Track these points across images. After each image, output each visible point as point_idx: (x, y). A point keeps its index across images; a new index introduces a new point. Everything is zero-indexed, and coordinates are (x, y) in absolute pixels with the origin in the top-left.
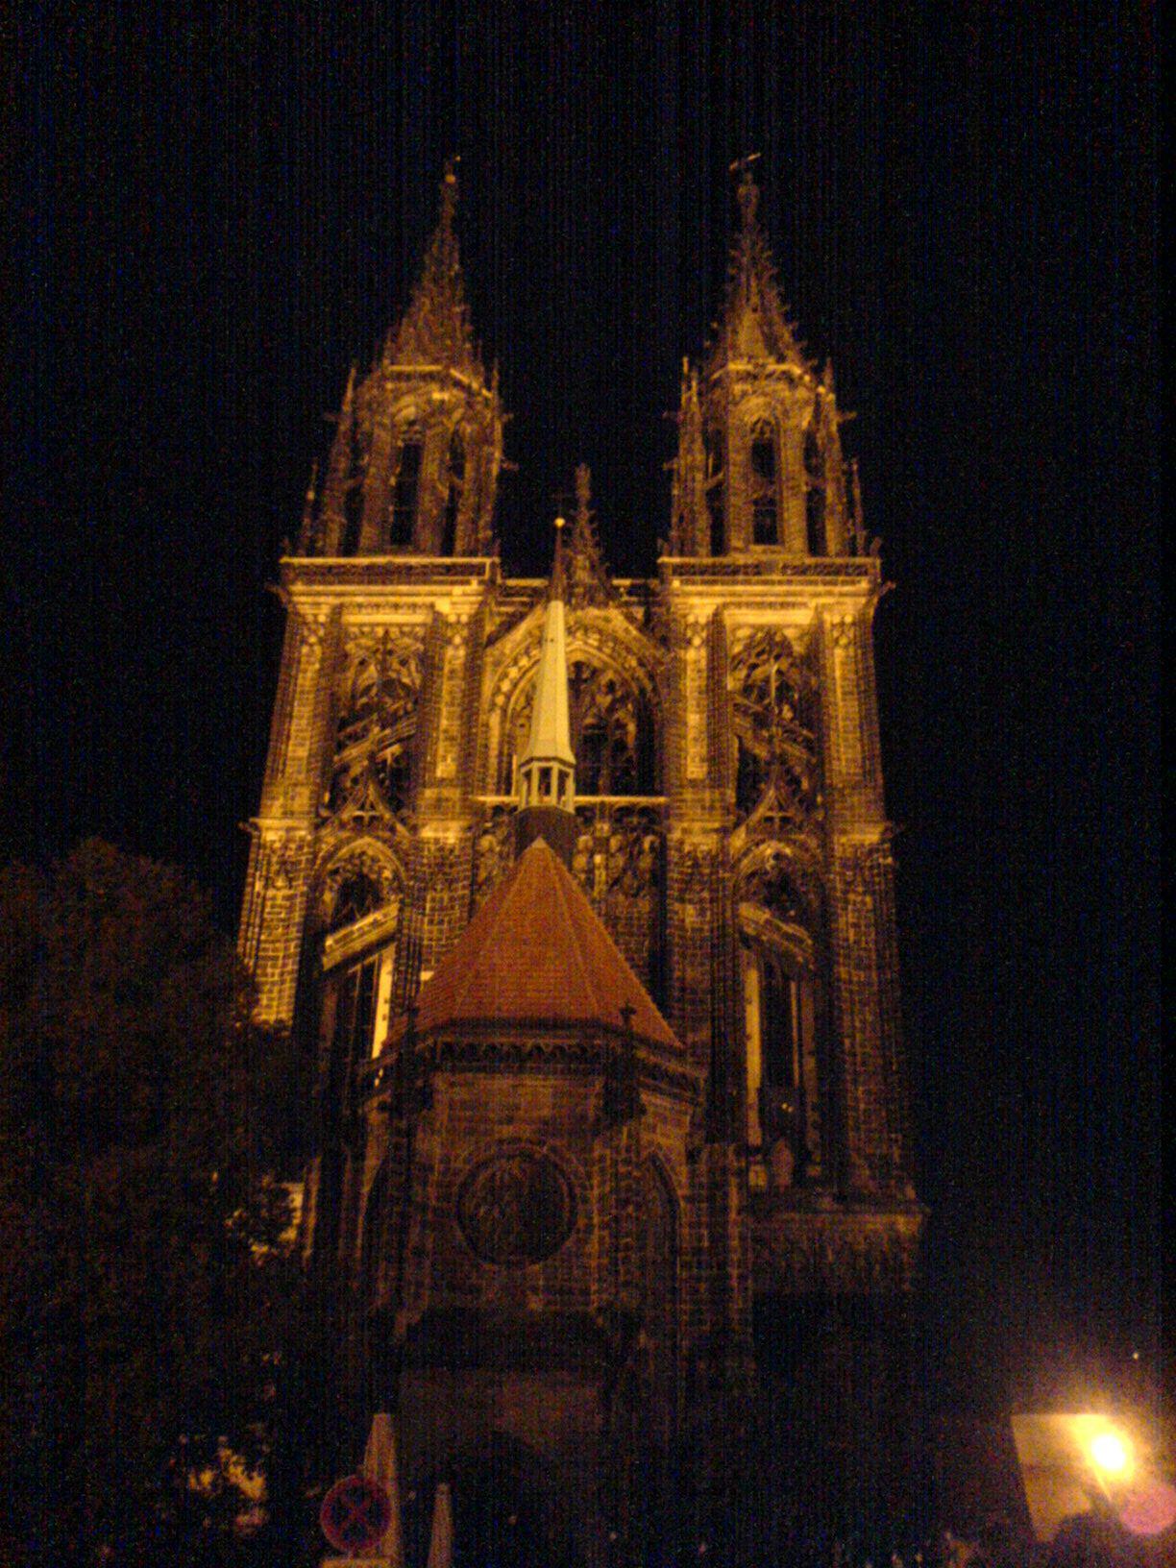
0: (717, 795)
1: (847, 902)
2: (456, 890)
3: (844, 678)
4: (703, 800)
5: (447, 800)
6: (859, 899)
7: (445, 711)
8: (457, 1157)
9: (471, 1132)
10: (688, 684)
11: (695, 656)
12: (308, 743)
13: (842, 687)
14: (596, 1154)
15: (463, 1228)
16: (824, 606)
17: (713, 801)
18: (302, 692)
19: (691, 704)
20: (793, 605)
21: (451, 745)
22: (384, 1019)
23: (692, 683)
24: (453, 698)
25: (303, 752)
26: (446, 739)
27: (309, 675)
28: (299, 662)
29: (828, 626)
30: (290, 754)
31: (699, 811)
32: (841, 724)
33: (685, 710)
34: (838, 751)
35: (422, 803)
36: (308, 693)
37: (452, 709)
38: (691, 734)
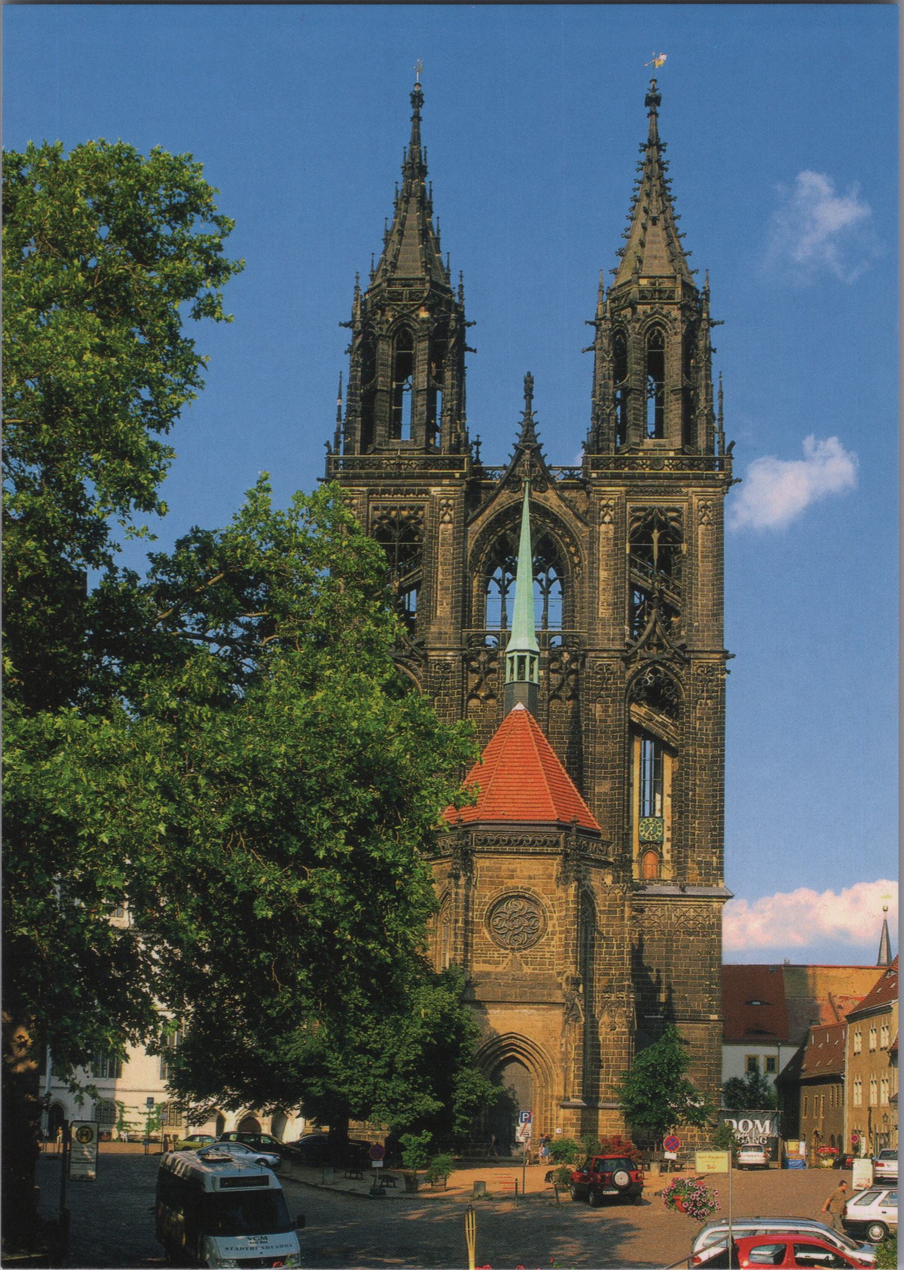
0: (617, 631)
1: (696, 703)
2: (453, 694)
4: (609, 634)
5: (446, 633)
7: (440, 568)
9: (492, 883)
10: (601, 549)
11: (606, 530)
15: (490, 932)
19: (602, 563)
23: (603, 548)
26: (441, 590)
29: (695, 507)
31: (606, 642)
34: (697, 599)
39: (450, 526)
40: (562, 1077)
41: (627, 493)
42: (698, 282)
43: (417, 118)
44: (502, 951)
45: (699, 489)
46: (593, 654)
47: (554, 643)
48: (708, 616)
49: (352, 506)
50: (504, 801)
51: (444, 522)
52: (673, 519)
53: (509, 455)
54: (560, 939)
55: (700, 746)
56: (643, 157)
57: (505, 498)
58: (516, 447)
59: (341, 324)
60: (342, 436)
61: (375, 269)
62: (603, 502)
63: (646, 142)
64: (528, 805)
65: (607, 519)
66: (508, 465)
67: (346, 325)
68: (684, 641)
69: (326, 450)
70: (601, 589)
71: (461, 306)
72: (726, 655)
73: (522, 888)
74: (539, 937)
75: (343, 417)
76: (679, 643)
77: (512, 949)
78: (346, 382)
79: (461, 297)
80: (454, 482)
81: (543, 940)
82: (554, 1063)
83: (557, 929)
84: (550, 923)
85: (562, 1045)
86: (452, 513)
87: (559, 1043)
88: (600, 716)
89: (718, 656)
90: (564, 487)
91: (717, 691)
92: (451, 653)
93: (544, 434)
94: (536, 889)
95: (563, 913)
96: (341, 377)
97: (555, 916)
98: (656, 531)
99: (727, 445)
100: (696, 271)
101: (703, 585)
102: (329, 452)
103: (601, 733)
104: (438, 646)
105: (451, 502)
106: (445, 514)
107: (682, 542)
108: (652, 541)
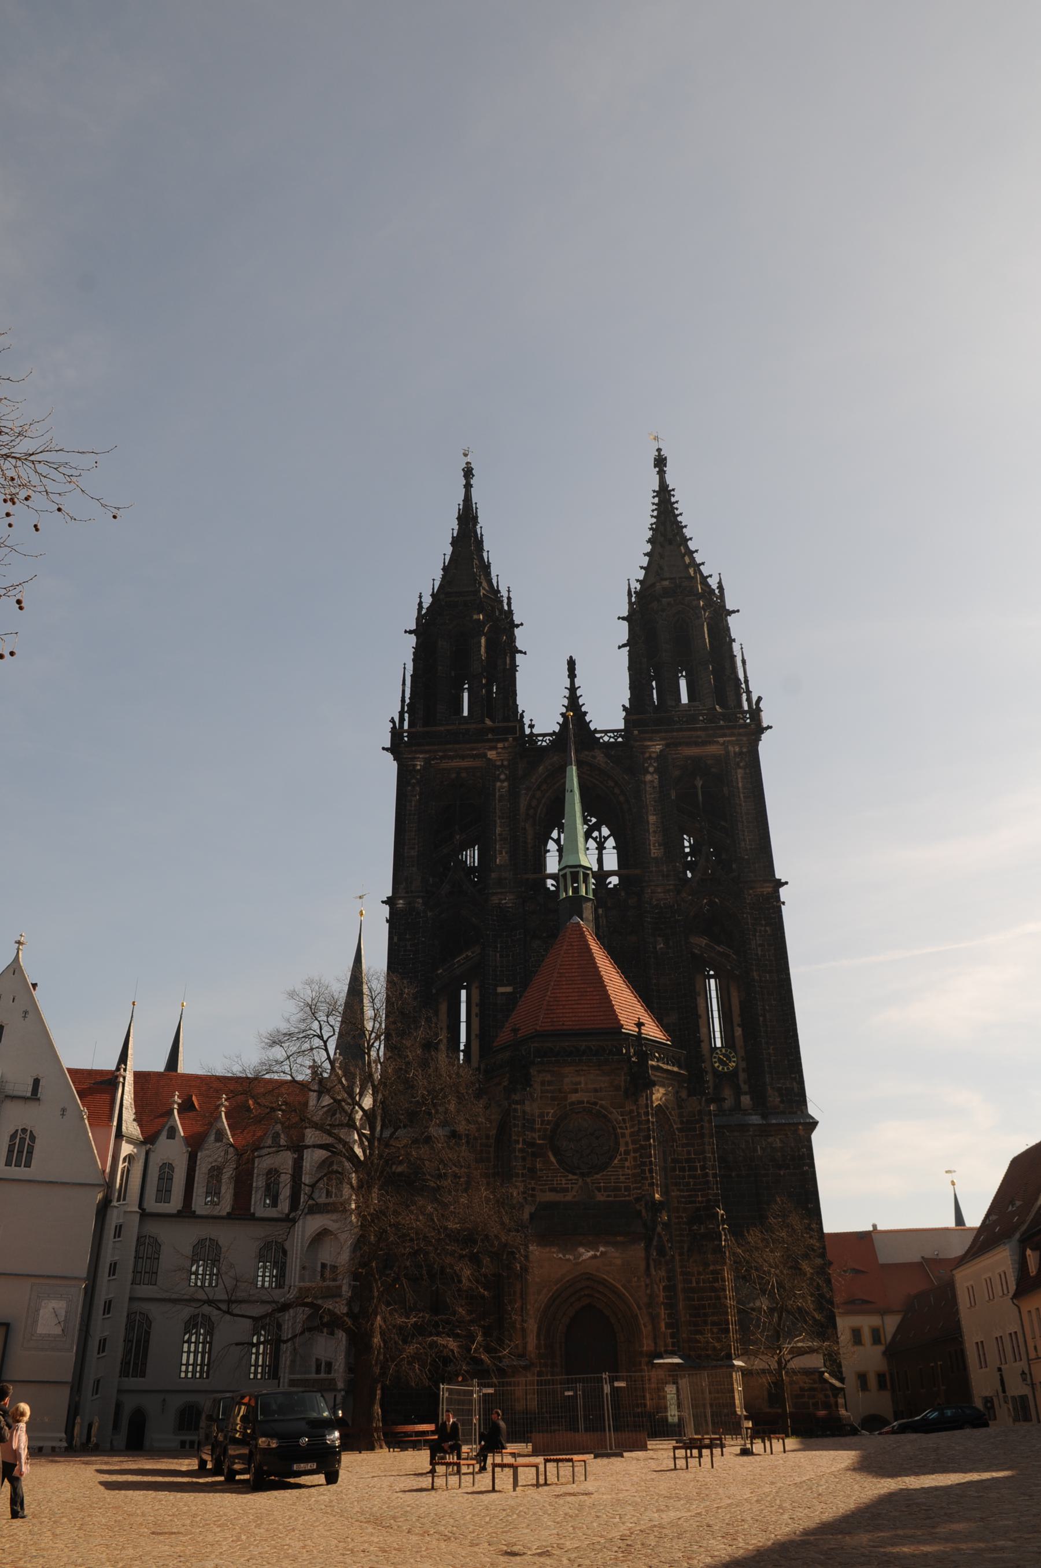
6: (763, 929)
7: (498, 821)
8: (548, 1113)
12: (417, 846)
13: (744, 793)
14: (627, 1109)
15: (555, 1156)
16: (729, 741)
19: (651, 808)
20: (710, 743)
22: (477, 1016)
23: (650, 797)
25: (414, 853)
27: (413, 803)
34: (744, 835)
37: (503, 821)
39: (505, 784)
40: (650, 1327)
41: (667, 745)
42: (713, 583)
43: (468, 486)
44: (571, 1177)
45: (734, 739)
47: (610, 883)
50: (564, 1011)
53: (558, 723)
54: (635, 1159)
56: (656, 500)
58: (563, 715)
59: (406, 632)
60: (406, 715)
61: (435, 591)
62: (647, 755)
63: (657, 489)
64: (589, 1014)
65: (651, 769)
66: (557, 731)
67: (410, 632)
69: (391, 725)
71: (510, 612)
72: (780, 884)
73: (588, 1102)
74: (612, 1158)
75: (407, 701)
77: (583, 1175)
78: (410, 671)
79: (509, 604)
80: (506, 744)
81: (616, 1161)
82: (640, 1308)
83: (631, 1147)
84: (622, 1141)
85: (647, 1286)
86: (507, 772)
87: (643, 1284)
88: (661, 948)
89: (771, 885)
93: (588, 703)
94: (603, 1102)
95: (636, 1129)
96: (405, 668)
97: (627, 1132)
98: (698, 778)
99: (754, 702)
100: (710, 576)
102: (394, 728)
104: (499, 891)
105: (506, 763)
106: (499, 775)
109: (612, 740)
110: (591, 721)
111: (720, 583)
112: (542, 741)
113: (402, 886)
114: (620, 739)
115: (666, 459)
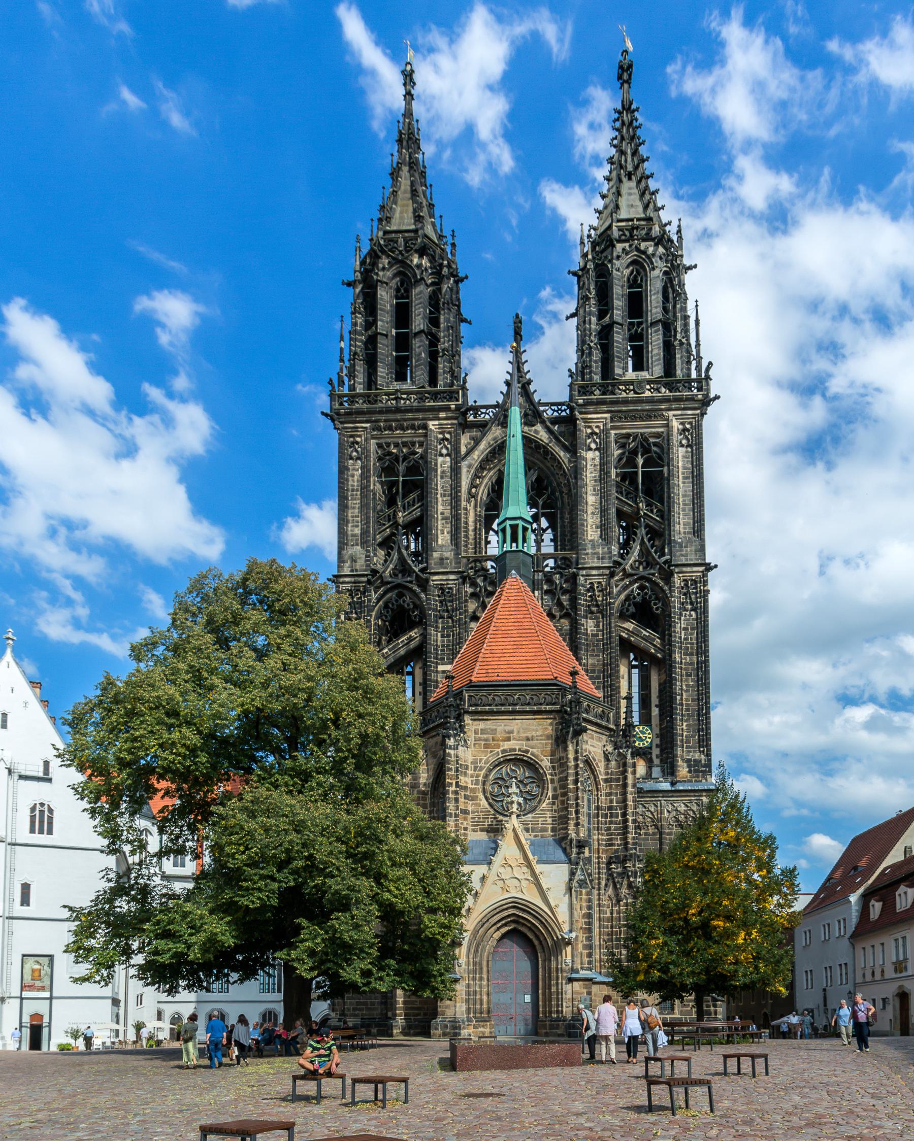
1: (681, 615)
3: (684, 468)
4: (598, 553)
5: (447, 559)
7: (440, 499)
10: (588, 475)
13: (683, 473)
17: (603, 553)
18: (353, 490)
19: (590, 489)
21: (447, 523)
23: (590, 475)
24: (445, 491)
25: (357, 531)
27: (356, 478)
28: (348, 469)
30: (350, 533)
32: (681, 500)
33: (586, 493)
35: (432, 562)
36: (357, 490)
38: (590, 509)
39: (448, 459)
42: (672, 230)
46: (584, 572)
47: (547, 565)
48: (689, 533)
49: (357, 443)
51: (441, 455)
52: (655, 444)
53: (502, 392)
55: (686, 654)
57: (495, 432)
58: (508, 383)
62: (589, 431)
68: (668, 557)
70: (589, 512)
72: (709, 568)
76: (663, 559)
88: (592, 631)
89: (701, 569)
90: (555, 421)
91: (700, 603)
92: (452, 577)
101: (684, 505)
103: (594, 646)
105: (448, 436)
107: (663, 466)
108: (636, 466)
109: (556, 414)
110: (535, 391)
111: (679, 231)
112: (486, 413)
113: (347, 565)
114: (564, 414)
115: (630, 66)
